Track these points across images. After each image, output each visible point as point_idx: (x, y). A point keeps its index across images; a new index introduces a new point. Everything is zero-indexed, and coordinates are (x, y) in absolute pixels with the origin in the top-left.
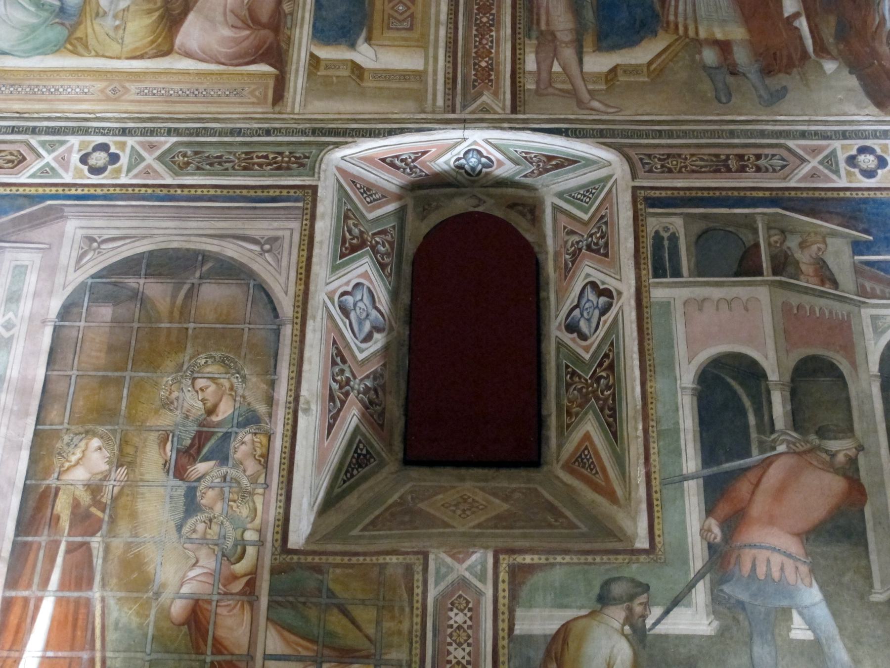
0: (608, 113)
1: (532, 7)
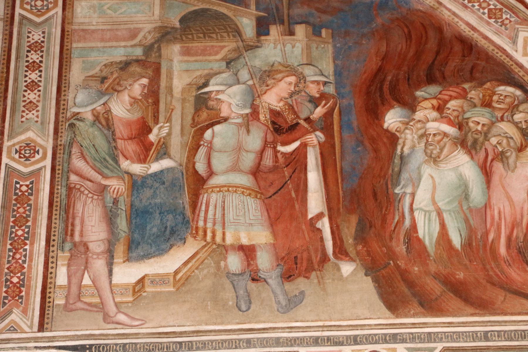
0: (132, 327)
1: (68, 217)
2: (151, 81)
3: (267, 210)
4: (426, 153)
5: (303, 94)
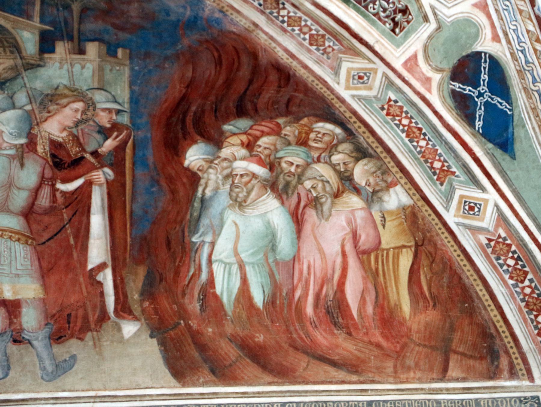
3: (39, 259)
5: (91, 123)
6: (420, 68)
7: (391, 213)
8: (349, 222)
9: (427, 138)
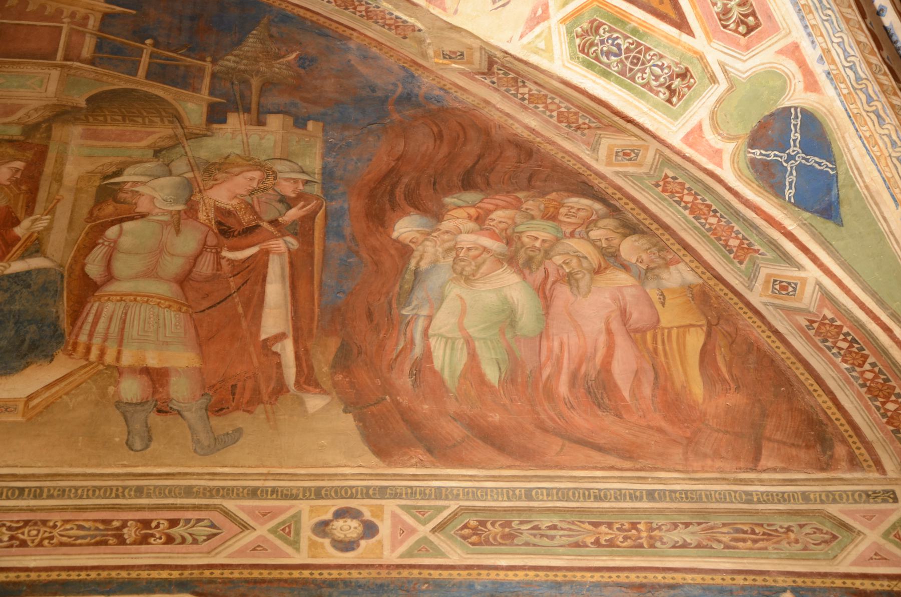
2: (29, 165)
3: (196, 327)
4: (454, 270)
5: (271, 192)
6: (707, 140)
7: (673, 291)
8: (615, 299)
9: (718, 215)
